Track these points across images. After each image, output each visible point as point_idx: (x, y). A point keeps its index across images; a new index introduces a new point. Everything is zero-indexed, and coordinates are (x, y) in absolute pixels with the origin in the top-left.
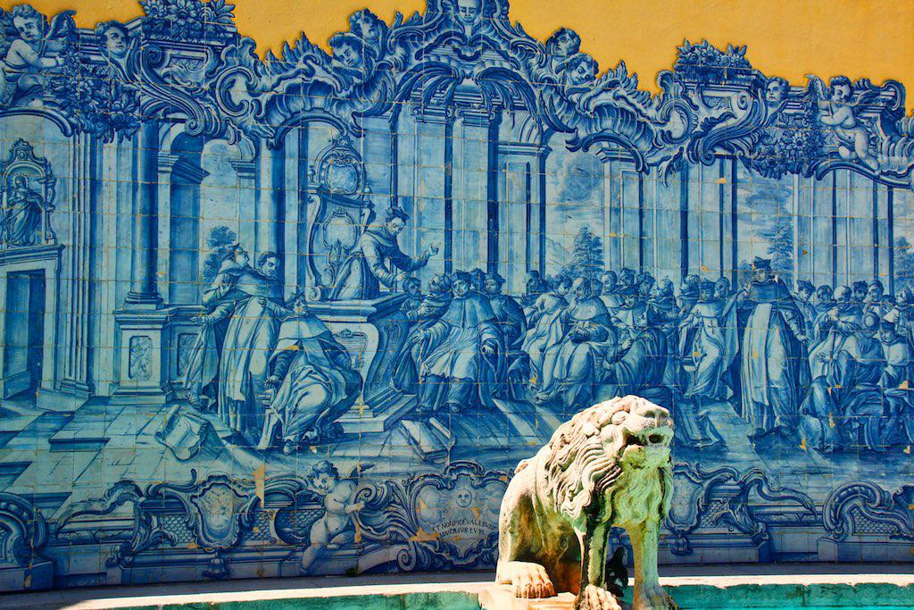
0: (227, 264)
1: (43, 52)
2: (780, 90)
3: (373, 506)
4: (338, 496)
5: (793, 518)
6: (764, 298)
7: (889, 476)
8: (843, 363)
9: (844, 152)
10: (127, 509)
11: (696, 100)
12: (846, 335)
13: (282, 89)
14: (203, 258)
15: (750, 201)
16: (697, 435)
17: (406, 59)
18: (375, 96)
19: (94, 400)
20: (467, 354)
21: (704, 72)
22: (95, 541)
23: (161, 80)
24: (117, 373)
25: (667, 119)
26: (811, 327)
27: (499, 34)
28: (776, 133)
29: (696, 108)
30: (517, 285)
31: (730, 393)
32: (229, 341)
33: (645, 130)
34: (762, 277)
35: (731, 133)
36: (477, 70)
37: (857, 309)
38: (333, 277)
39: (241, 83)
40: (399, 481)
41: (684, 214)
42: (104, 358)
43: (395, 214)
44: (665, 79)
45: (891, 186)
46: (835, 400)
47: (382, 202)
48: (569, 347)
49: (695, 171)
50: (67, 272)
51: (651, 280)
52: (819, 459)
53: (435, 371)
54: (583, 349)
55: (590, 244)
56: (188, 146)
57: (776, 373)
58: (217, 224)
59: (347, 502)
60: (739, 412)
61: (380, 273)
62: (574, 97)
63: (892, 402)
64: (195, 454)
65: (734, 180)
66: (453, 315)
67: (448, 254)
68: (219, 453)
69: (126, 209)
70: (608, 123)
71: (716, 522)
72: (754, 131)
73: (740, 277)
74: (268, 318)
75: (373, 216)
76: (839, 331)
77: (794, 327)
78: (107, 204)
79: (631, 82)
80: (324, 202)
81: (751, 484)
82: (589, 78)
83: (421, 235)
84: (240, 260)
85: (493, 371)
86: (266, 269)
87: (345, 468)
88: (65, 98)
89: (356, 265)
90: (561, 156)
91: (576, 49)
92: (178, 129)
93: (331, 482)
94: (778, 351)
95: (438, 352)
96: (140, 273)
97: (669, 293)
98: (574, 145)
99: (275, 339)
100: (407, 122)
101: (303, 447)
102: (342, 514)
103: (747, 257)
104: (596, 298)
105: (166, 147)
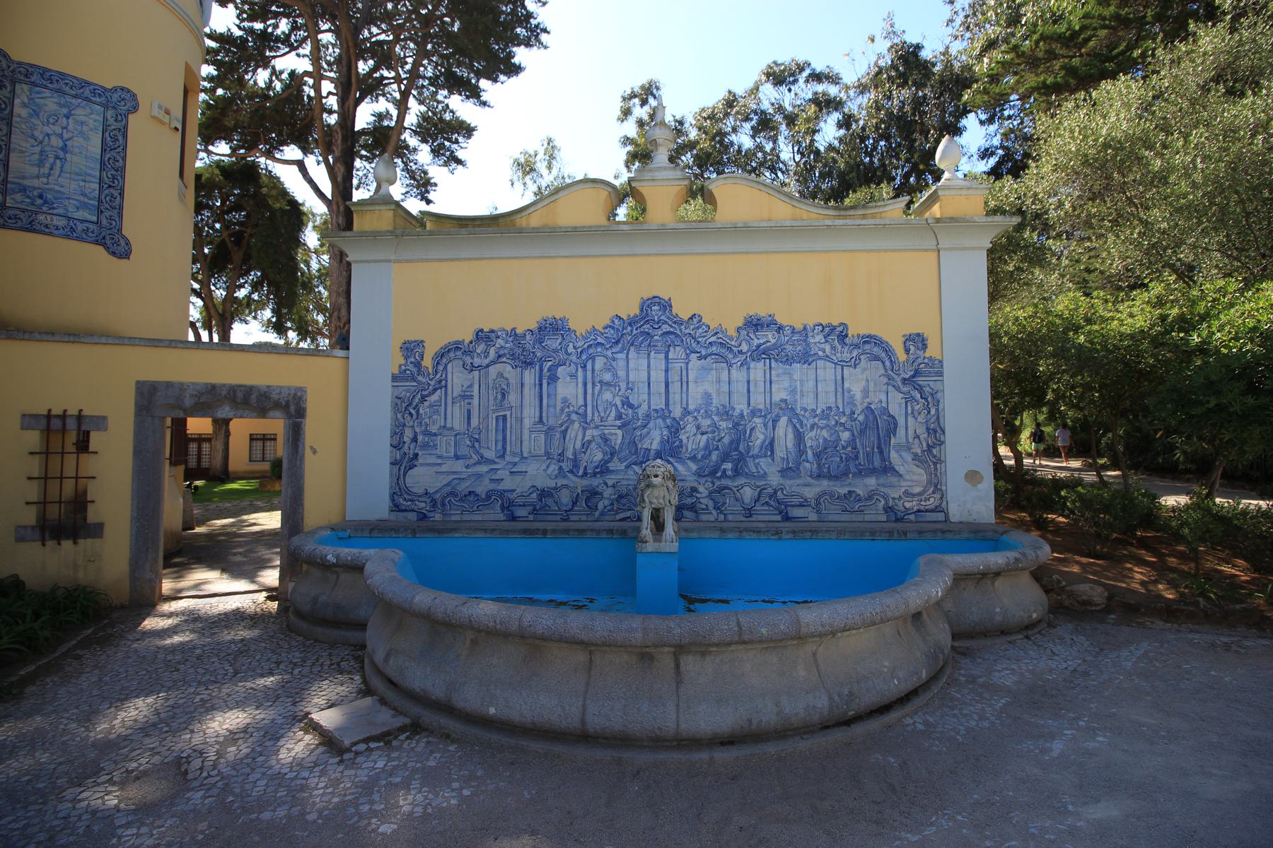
0: (567, 410)
1: (506, 343)
2: (791, 330)
3: (621, 497)
4: (608, 493)
5: (798, 503)
6: (785, 415)
7: (842, 486)
8: (821, 441)
9: (820, 353)
10: (534, 495)
11: (753, 336)
12: (822, 428)
13: (586, 346)
14: (558, 408)
15: (778, 376)
16: (754, 470)
17: (632, 331)
18: (620, 345)
19: (523, 458)
20: (658, 439)
21: (756, 325)
22: (524, 505)
23: (544, 347)
24: (530, 449)
25: (740, 345)
26: (806, 425)
27: (668, 318)
28: (789, 348)
29: (752, 339)
30: (677, 412)
31: (769, 453)
32: (567, 438)
33: (729, 349)
34: (784, 406)
35: (769, 349)
36: (660, 333)
37: (827, 417)
38: (605, 413)
39: (571, 345)
40: (631, 487)
41: (748, 382)
42: (526, 443)
43: (628, 388)
44: (738, 330)
45: (842, 366)
46: (817, 456)
47: (623, 386)
48: (699, 436)
49: (752, 364)
50: (514, 415)
51: (734, 409)
52: (809, 480)
53: (645, 446)
54: (705, 437)
55: (707, 396)
57: (790, 445)
58: (562, 396)
59: (611, 495)
60: (773, 461)
61: (623, 411)
62: (700, 340)
63: (844, 456)
64: (556, 477)
65: (770, 367)
66: (651, 425)
67: (649, 403)
68: (565, 477)
69: (533, 392)
70: (714, 348)
71: (763, 504)
73: (773, 406)
74: (581, 428)
75: (620, 390)
76: (818, 427)
77: (798, 426)
78: (526, 391)
79: (724, 332)
80: (601, 386)
81: (779, 490)
82: (706, 332)
83: (638, 396)
84: (571, 408)
85: (667, 447)
86: (581, 411)
87: (610, 483)
88: (513, 356)
89: (614, 408)
91: (700, 321)
92: (550, 363)
93: (605, 487)
94: (791, 436)
95: (645, 439)
96: (537, 414)
97: (742, 415)
98: (700, 358)
99: (584, 436)
100: (632, 354)
101: (595, 475)
102: (609, 499)
103: (776, 398)
104: (710, 417)
105: (545, 370)
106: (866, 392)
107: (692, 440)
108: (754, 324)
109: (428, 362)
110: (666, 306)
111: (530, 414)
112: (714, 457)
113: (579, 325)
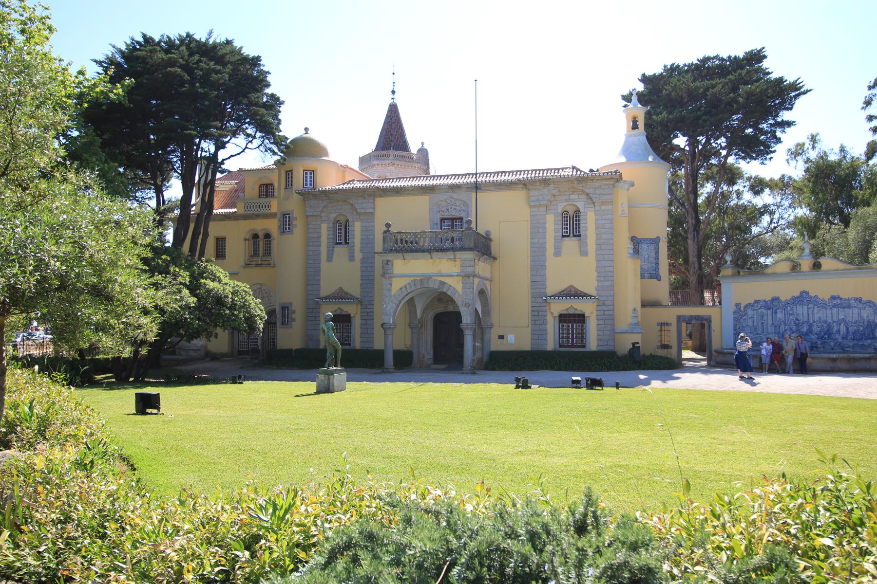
30: (811, 322)
46: (853, 334)
55: (820, 318)
56: (776, 310)
72: (841, 304)
88: (765, 307)
90: (816, 309)
103: (840, 318)
106: (868, 317)
107: (815, 329)
108: (833, 298)
109: (742, 309)
110: (807, 293)
111: (770, 322)
112: (822, 334)
113: (783, 298)
